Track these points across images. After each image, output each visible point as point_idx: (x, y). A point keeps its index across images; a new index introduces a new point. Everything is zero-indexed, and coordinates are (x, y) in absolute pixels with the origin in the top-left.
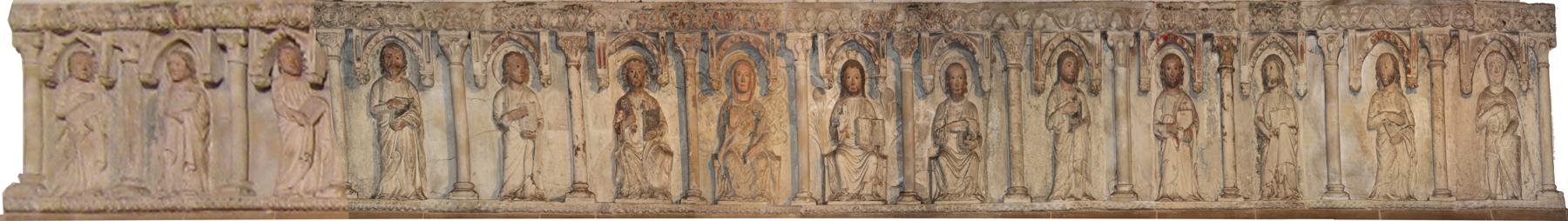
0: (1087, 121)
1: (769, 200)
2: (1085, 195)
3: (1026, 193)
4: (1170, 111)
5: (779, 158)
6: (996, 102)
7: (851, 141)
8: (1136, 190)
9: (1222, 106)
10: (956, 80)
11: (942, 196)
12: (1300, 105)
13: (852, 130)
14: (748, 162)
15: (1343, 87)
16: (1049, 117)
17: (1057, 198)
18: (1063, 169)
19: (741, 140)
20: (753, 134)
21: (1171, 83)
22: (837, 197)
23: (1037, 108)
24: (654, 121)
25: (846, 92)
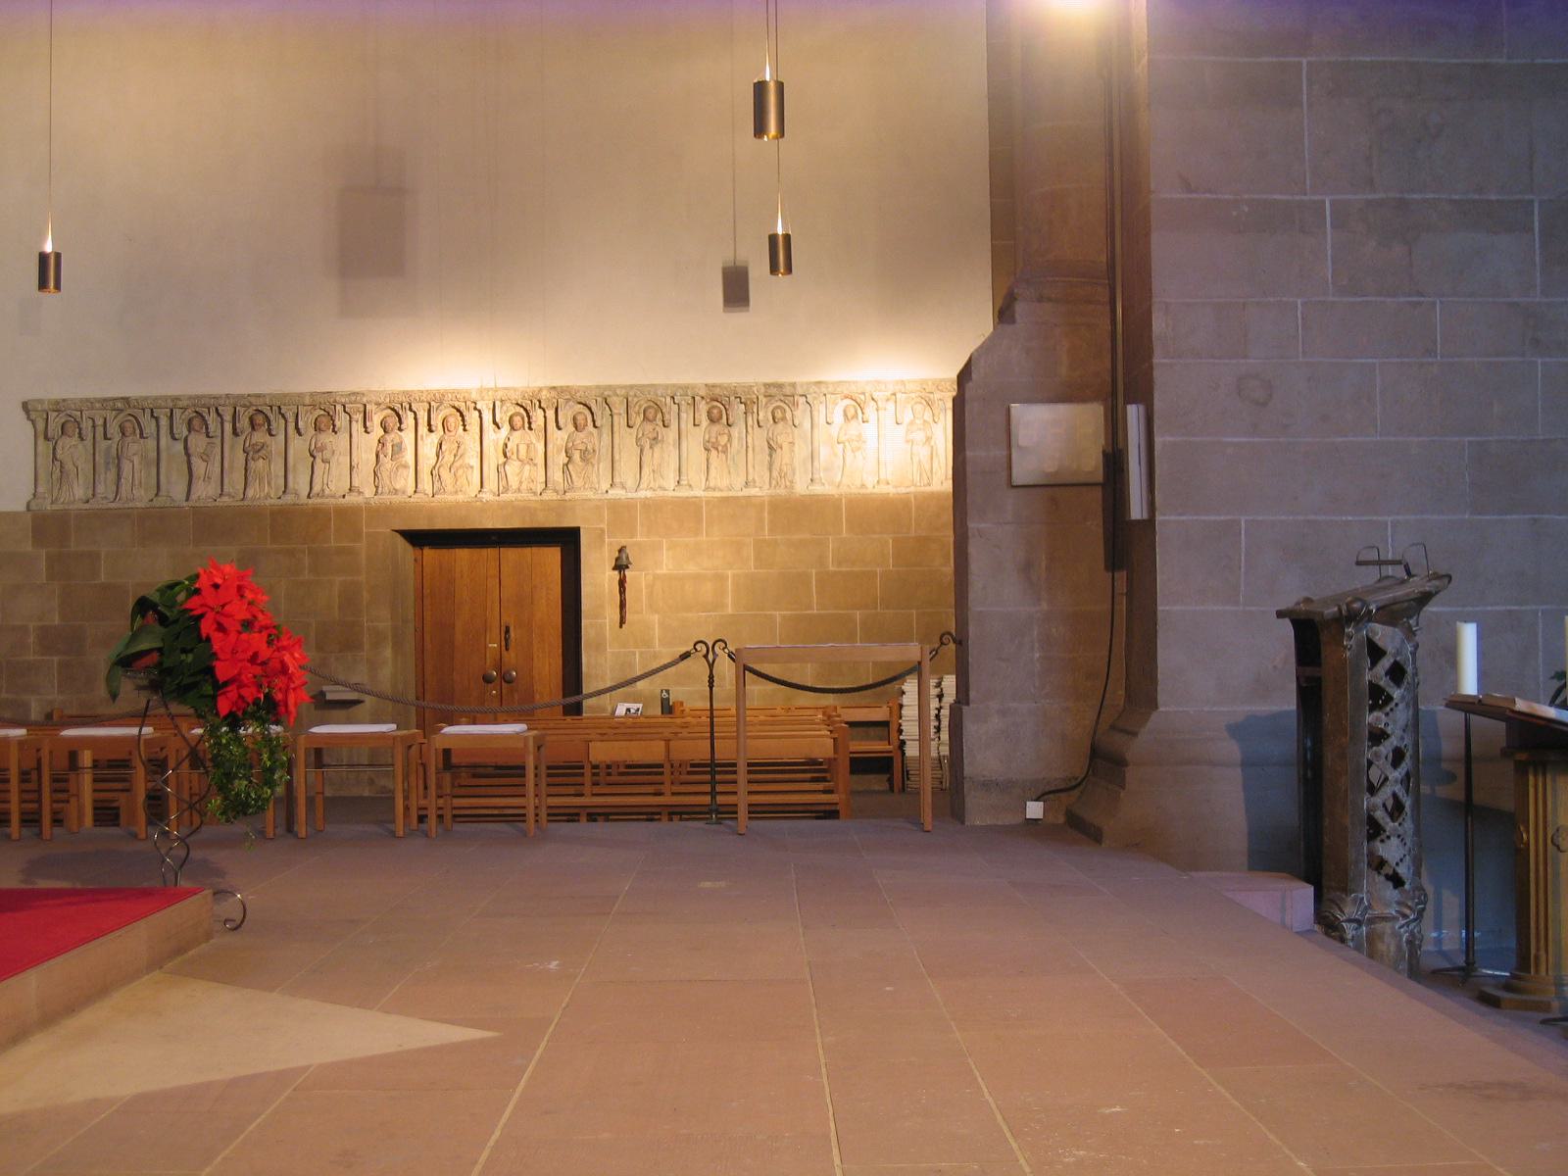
0: (663, 441)
1: (465, 494)
2: (660, 487)
3: (624, 487)
4: (714, 435)
5: (472, 467)
6: (606, 431)
7: (515, 457)
8: (691, 483)
9: (747, 431)
10: (580, 418)
11: (571, 488)
12: (796, 430)
13: (515, 451)
14: (452, 471)
15: (820, 419)
16: (638, 440)
17: (642, 490)
18: (646, 470)
19: (448, 458)
20: (455, 456)
21: (712, 420)
22: (506, 490)
23: (630, 434)
24: (398, 448)
25: (513, 428)
